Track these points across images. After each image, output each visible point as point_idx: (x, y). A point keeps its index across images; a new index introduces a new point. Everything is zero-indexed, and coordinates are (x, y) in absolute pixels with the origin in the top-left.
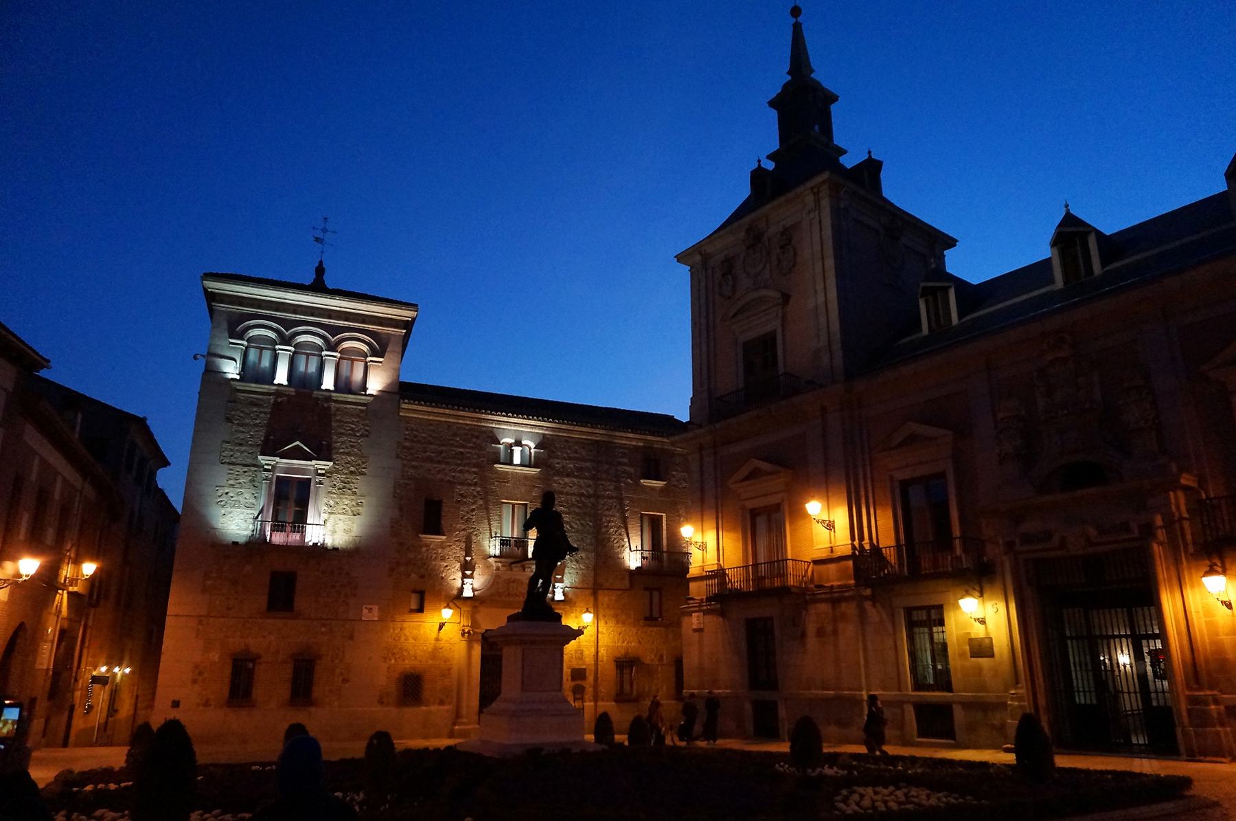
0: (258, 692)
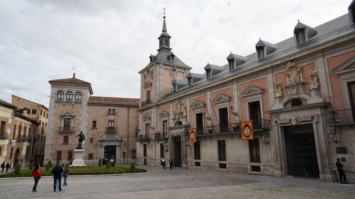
0: (62, 158)
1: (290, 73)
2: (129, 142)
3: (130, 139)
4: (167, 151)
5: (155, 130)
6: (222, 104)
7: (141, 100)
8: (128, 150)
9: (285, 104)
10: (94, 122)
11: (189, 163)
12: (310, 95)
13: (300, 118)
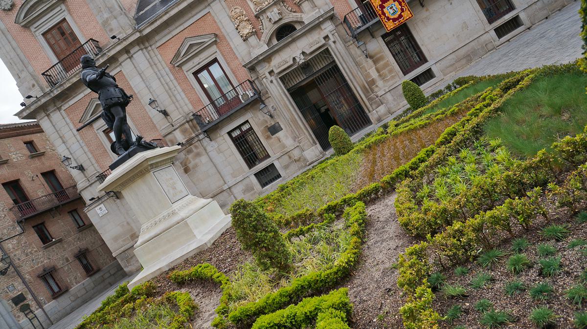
2: (12, 255)
4: (274, 130)
8: (24, 282)
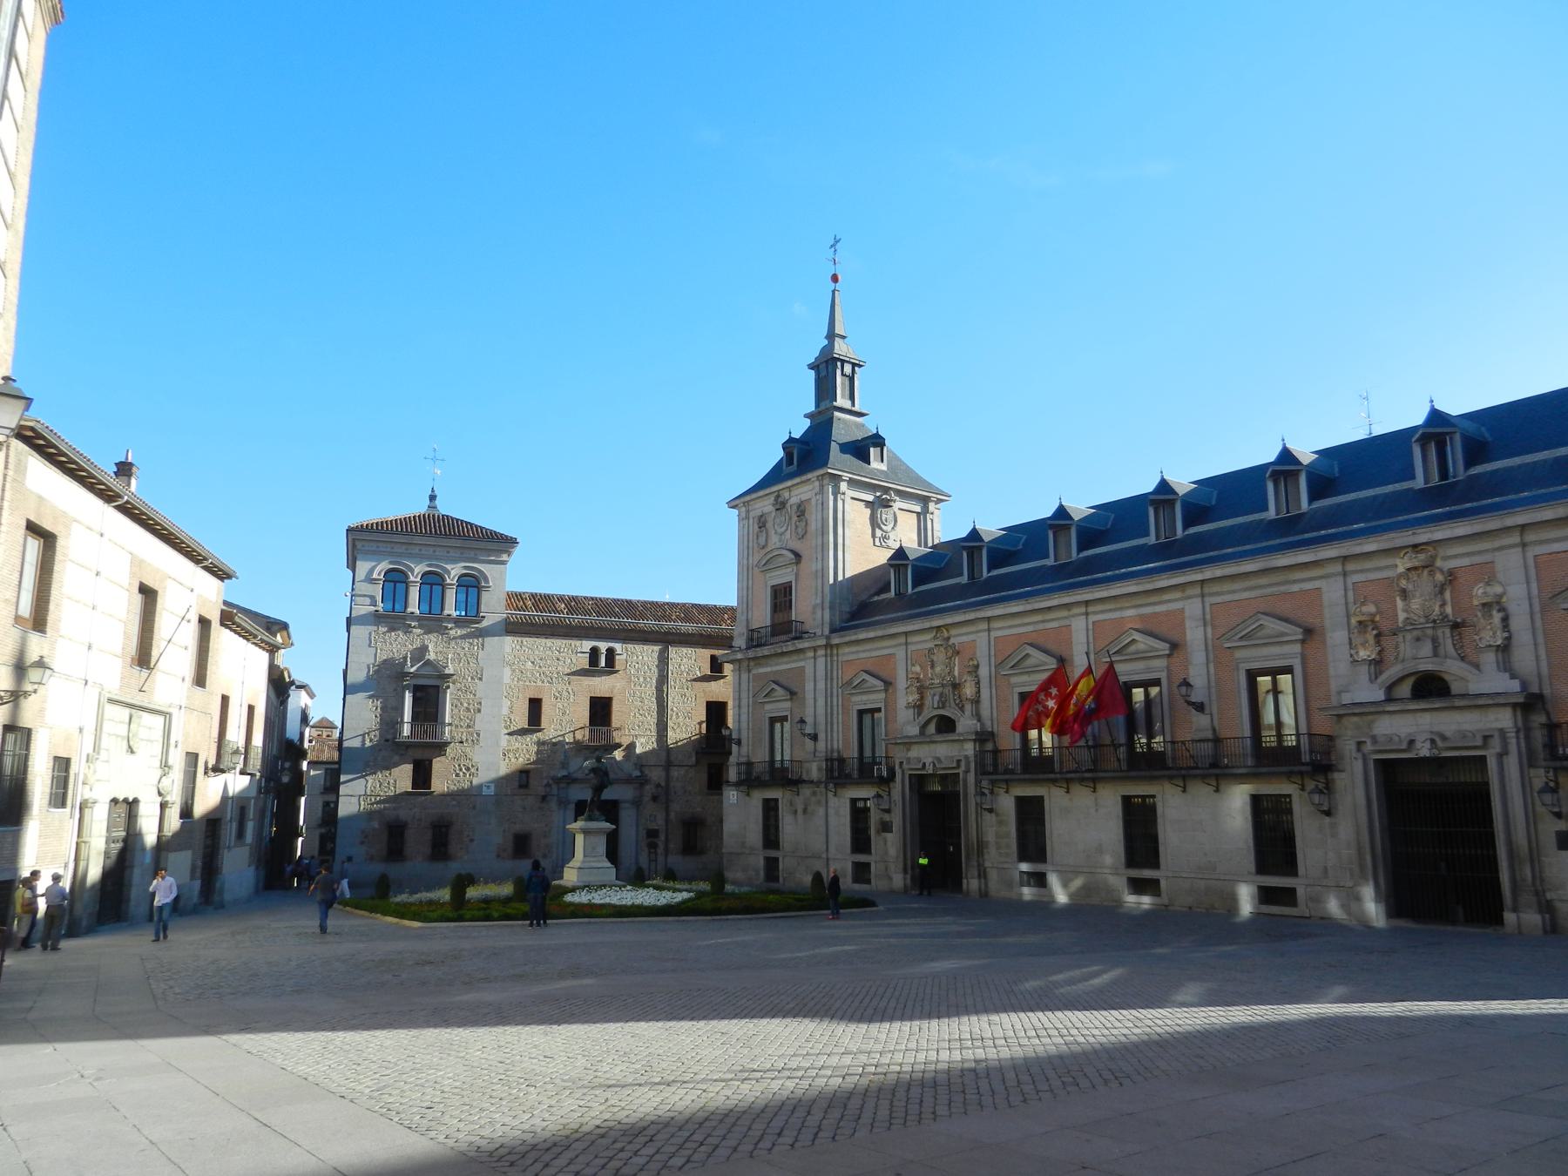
1: (1410, 587)
3: (675, 773)
4: (886, 827)
5: (821, 745)
6: (1140, 665)
7: (741, 617)
8: (667, 821)
9: (1390, 688)
10: (531, 700)
11: (993, 875)
12: (1477, 666)
13: (1444, 738)
